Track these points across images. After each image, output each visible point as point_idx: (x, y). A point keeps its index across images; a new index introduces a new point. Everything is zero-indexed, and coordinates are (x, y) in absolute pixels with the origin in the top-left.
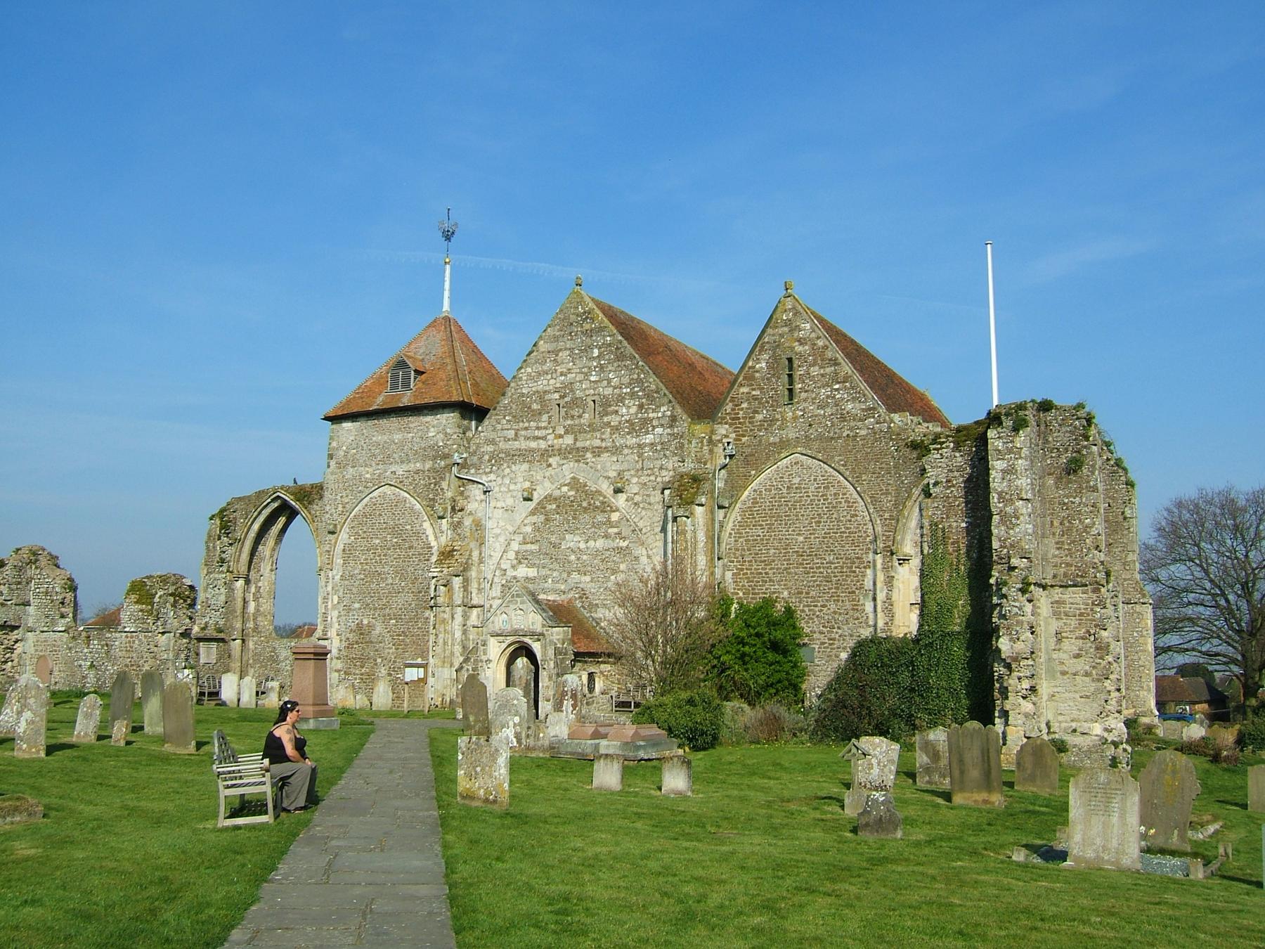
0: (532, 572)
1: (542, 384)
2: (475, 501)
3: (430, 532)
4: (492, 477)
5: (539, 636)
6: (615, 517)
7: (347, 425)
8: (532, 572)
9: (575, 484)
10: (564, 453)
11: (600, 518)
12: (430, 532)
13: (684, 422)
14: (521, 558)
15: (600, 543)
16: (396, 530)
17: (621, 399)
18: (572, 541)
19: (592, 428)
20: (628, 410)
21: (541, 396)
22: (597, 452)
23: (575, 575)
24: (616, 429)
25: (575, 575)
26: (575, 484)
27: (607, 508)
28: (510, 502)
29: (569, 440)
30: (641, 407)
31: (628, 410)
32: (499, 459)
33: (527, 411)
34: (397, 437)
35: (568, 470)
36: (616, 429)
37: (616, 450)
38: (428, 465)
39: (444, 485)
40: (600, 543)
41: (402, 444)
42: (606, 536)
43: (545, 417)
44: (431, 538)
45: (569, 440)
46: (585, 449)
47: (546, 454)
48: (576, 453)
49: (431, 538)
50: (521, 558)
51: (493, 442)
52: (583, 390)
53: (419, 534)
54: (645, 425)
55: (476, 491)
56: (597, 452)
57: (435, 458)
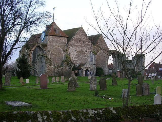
0: (76, 60)
1: (78, 37)
2: (69, 51)
3: (63, 53)
4: (72, 47)
5: (90, 68)
6: (85, 54)
7: (51, 36)
8: (76, 60)
9: (81, 50)
10: (80, 46)
11: (84, 54)
12: (63, 53)
13: (92, 45)
14: (75, 58)
15: (84, 57)
16: (58, 52)
17: (86, 41)
18: (81, 56)
19: (83, 44)
20: (87, 43)
21: (78, 39)
22: (84, 47)
23: (81, 60)
24: (86, 44)
25: (81, 60)
26: (81, 50)
27: (85, 53)
28: (74, 51)
29: (81, 45)
30: (88, 43)
31: (87, 43)
32: (72, 45)
33: (76, 40)
34: (59, 40)
35: (81, 48)
36: (86, 44)
37: (86, 47)
38: (63, 44)
39: (65, 47)
40: (84, 57)
41: (59, 41)
42: (84, 56)
43: (78, 41)
44: (63, 54)
45: (81, 45)
46: (83, 46)
47: (78, 46)
48: (82, 46)
49: (63, 54)
50: (75, 58)
51: (72, 43)
52: (83, 39)
53: (62, 53)
54: (88, 45)
55: (70, 49)
56: (84, 47)
57: (64, 44)
